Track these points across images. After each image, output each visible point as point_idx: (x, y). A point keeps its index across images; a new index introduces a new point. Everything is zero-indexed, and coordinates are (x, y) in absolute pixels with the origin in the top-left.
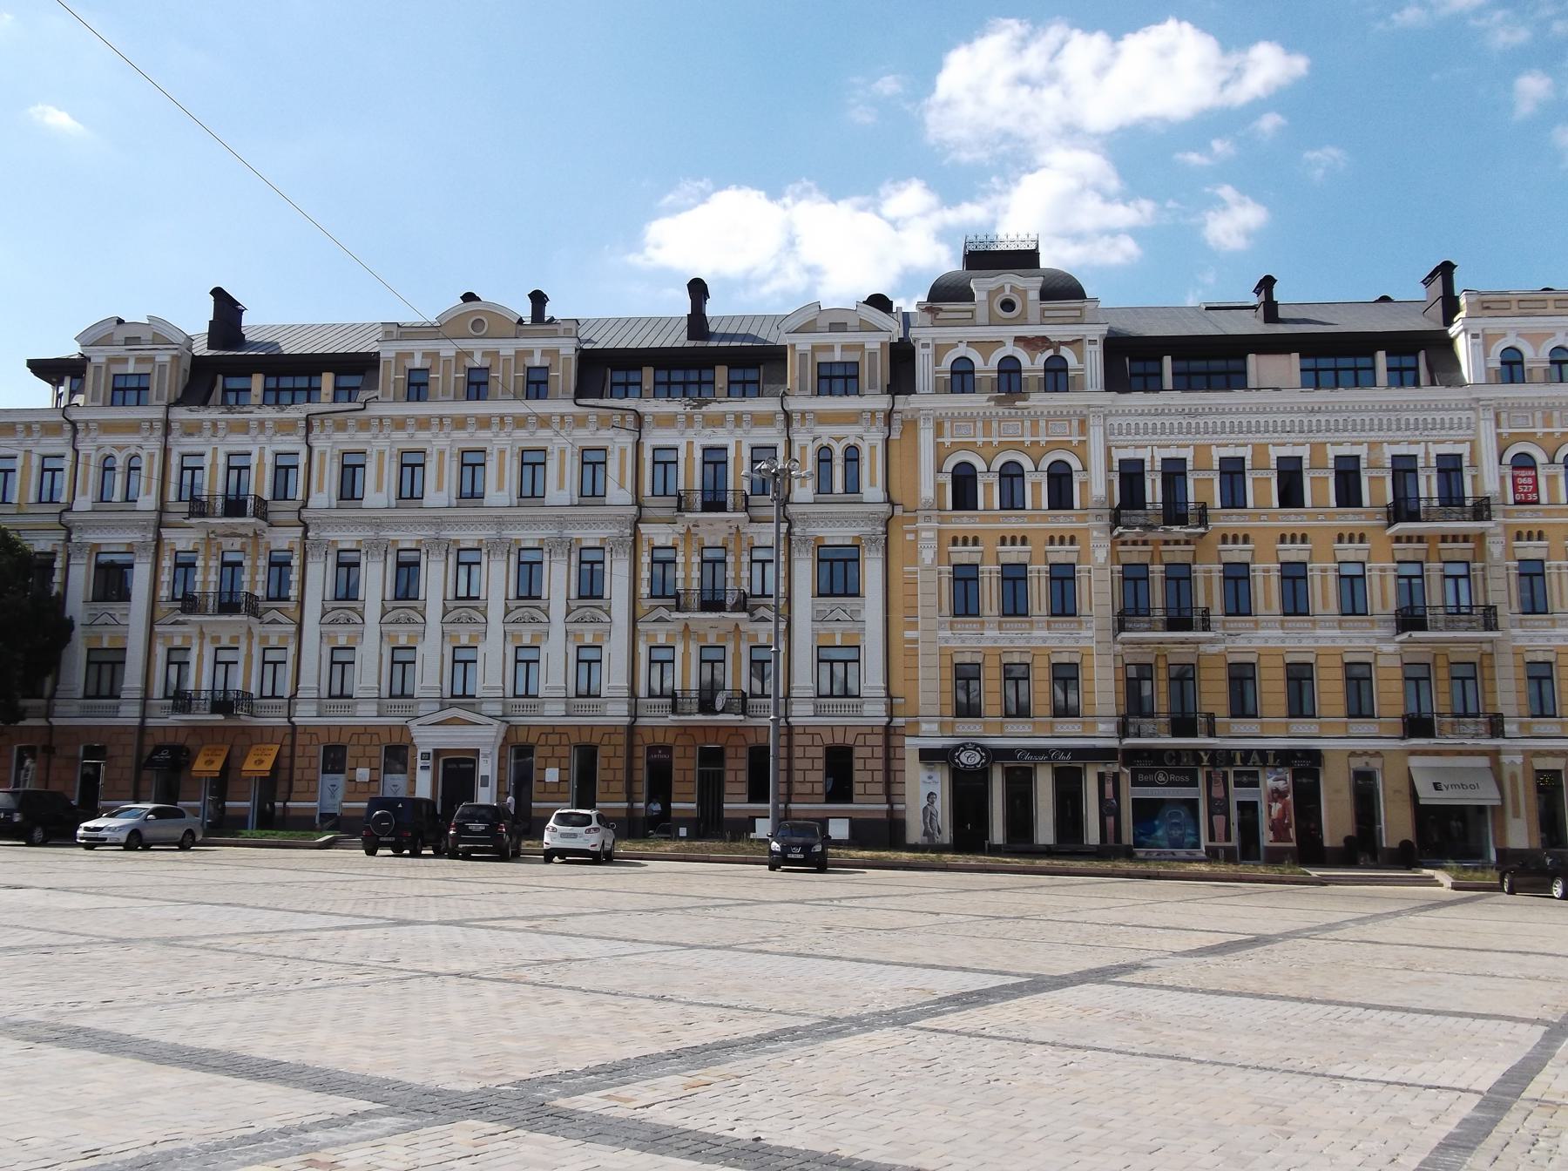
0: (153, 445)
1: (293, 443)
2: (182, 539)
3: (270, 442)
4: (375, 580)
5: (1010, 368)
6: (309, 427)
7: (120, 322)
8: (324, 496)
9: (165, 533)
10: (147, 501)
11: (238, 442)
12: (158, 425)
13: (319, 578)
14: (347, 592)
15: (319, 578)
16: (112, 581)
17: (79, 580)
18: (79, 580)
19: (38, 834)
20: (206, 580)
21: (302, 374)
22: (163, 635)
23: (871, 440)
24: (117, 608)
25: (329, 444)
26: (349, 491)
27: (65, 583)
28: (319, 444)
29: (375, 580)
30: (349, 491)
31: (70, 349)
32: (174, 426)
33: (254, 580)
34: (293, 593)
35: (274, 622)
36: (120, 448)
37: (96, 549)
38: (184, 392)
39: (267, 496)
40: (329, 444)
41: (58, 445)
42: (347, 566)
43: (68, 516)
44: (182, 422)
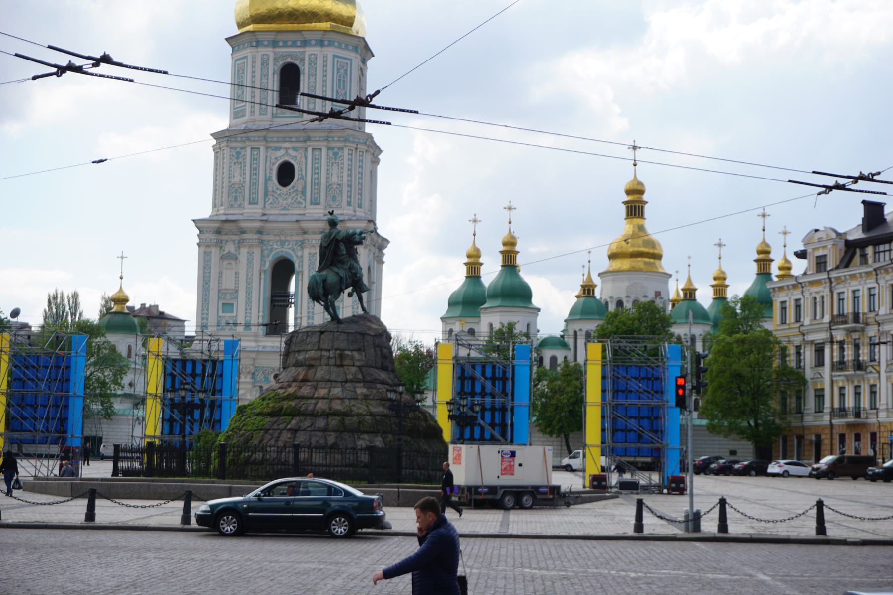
0: (826, 292)
1: (871, 283)
2: (839, 335)
3: (866, 283)
6: (877, 275)
7: (816, 230)
9: (834, 333)
10: (827, 319)
11: (854, 285)
12: (827, 281)
19: (753, 472)
21: (884, 243)
22: (837, 381)
24: (819, 369)
27: (799, 361)
28: (882, 282)
31: (800, 247)
32: (833, 280)
34: (877, 357)
35: (871, 372)
36: (817, 293)
37: (812, 342)
38: (842, 261)
39: (866, 311)
41: (797, 294)
43: (802, 328)
44: (836, 278)
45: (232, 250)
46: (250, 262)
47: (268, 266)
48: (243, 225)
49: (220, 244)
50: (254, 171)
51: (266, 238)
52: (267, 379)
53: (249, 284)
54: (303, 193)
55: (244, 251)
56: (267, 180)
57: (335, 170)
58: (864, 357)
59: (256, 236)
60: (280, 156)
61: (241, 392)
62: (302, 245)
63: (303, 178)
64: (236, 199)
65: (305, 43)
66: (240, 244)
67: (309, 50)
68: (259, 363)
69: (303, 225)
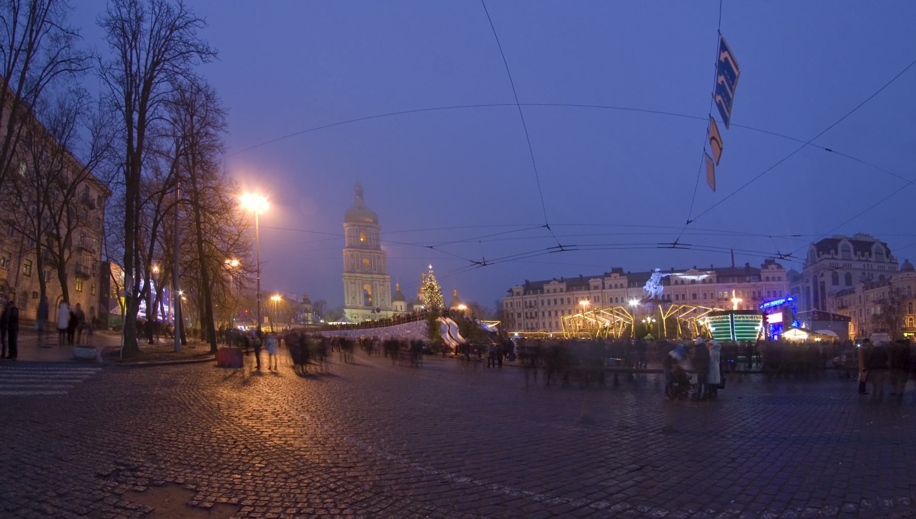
2: (526, 310)
4: (547, 314)
5: (616, 286)
8: (540, 304)
13: (540, 314)
14: (543, 315)
15: (540, 314)
16: (519, 315)
17: (516, 316)
18: (516, 316)
20: (529, 315)
23: (600, 295)
25: (540, 299)
26: (543, 304)
29: (547, 314)
30: (543, 304)
33: (534, 315)
40: (540, 299)
42: (543, 313)
58: (534, 315)
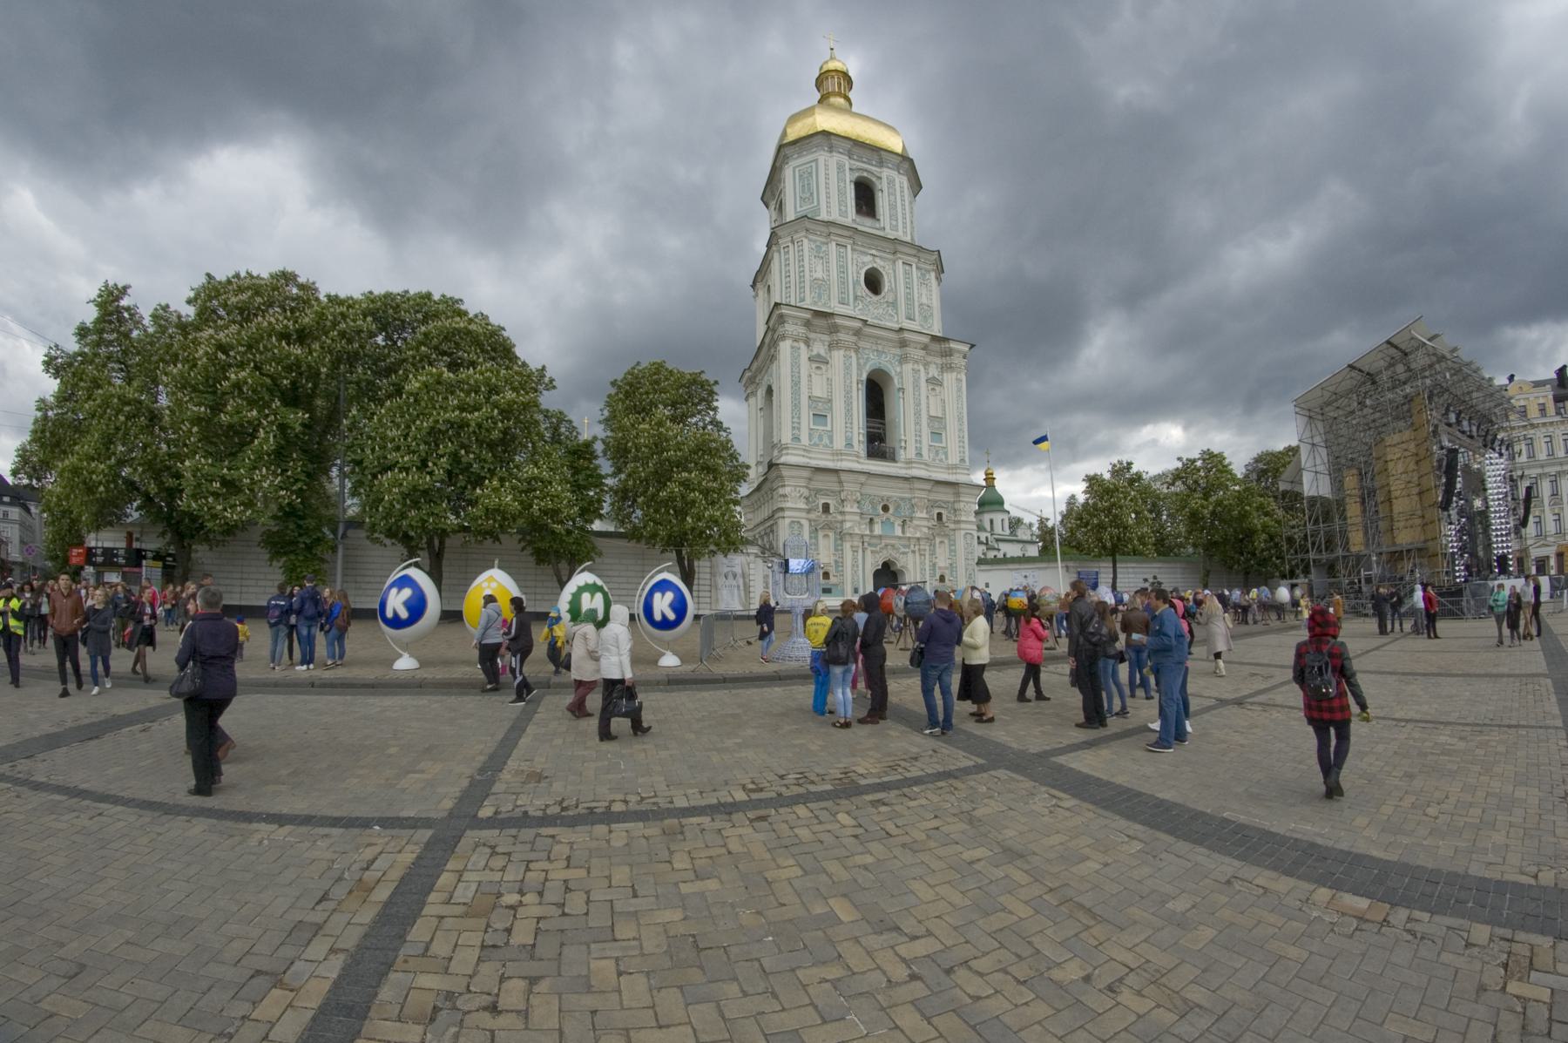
45: (822, 353)
46: (847, 368)
47: (864, 377)
48: (839, 321)
49: (807, 342)
50: (843, 270)
51: (861, 344)
52: (874, 508)
53: (848, 393)
54: (894, 304)
55: (838, 356)
56: (856, 283)
57: (924, 291)
59: (854, 339)
60: (868, 262)
61: (848, 525)
62: (903, 359)
63: (894, 291)
64: (820, 296)
65: (881, 164)
66: (832, 346)
67: (886, 173)
68: (867, 490)
69: (907, 335)
